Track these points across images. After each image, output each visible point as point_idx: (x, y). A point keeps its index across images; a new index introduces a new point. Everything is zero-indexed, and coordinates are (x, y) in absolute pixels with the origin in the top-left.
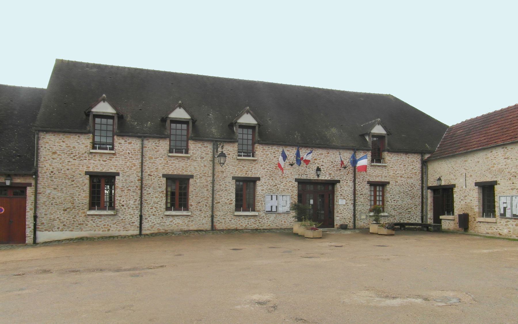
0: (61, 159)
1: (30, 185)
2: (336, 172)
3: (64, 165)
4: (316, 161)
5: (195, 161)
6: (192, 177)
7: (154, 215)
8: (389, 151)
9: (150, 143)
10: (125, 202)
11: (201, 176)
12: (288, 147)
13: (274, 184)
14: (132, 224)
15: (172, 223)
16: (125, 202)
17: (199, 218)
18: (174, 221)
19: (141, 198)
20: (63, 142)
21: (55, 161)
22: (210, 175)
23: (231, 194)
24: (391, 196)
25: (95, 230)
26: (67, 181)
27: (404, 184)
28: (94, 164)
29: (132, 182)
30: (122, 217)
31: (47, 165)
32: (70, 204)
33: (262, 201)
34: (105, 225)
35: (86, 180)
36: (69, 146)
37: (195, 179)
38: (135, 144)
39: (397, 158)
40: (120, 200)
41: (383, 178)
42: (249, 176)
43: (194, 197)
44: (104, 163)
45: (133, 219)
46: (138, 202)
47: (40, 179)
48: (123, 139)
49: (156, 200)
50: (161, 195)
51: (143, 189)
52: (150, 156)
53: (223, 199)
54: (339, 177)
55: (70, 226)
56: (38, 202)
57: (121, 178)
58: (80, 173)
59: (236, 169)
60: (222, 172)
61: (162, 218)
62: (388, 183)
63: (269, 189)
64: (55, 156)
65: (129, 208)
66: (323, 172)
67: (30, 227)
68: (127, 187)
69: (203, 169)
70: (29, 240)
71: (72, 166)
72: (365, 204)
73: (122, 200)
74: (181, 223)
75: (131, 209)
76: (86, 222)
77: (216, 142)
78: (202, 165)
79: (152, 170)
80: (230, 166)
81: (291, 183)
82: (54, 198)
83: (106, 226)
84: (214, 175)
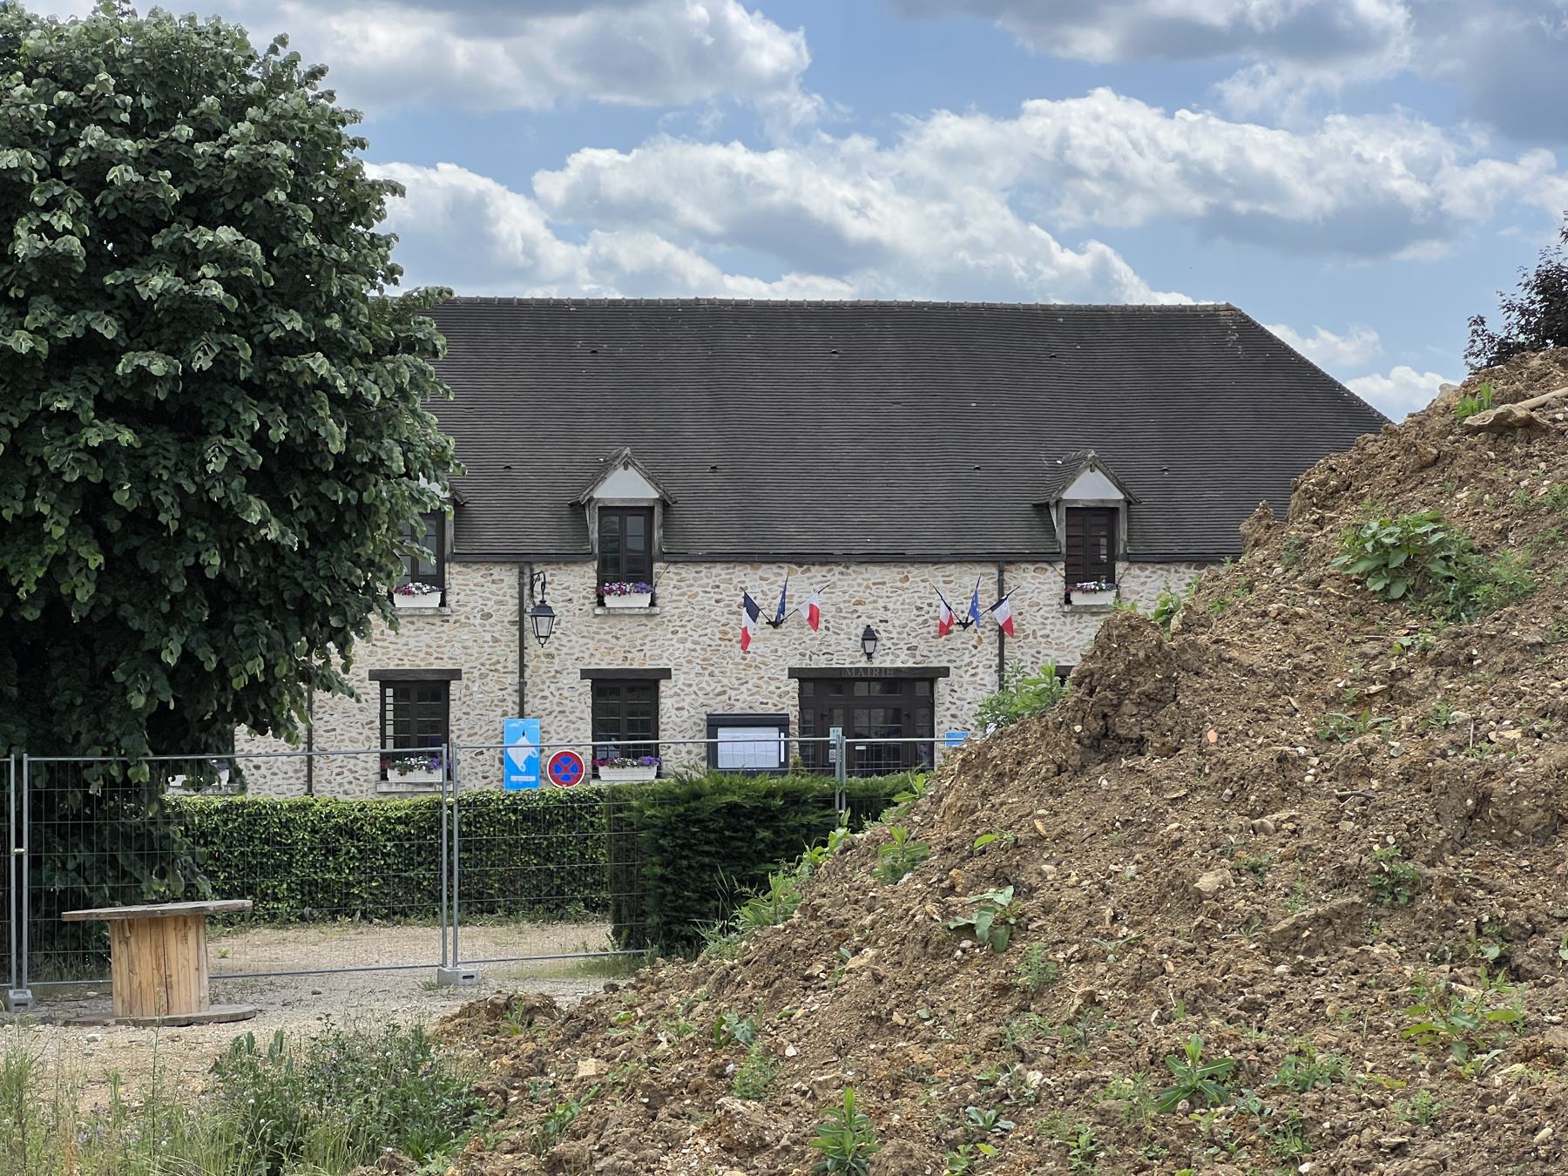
4: (859, 608)
6: (456, 674)
8: (1132, 559)
11: (483, 670)
12: (764, 566)
13: (719, 689)
23: (580, 724)
37: (464, 681)
42: (635, 666)
43: (464, 737)
50: (366, 732)
54: (945, 658)
59: (592, 644)
63: (703, 705)
66: (889, 644)
69: (489, 650)
75: (281, 775)
77: (524, 561)
78: (488, 637)
84: (522, 667)
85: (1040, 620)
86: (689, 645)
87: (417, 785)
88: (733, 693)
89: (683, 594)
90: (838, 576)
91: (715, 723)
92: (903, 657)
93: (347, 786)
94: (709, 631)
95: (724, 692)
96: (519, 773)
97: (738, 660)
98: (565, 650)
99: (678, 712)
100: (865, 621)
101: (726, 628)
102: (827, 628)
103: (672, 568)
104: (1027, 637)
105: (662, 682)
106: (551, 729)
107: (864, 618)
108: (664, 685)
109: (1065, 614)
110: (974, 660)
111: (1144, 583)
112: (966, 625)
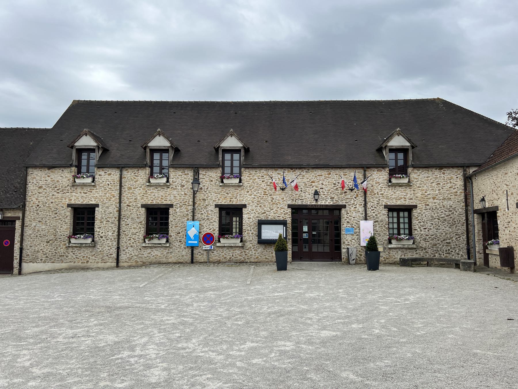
0: (46, 193)
1: (18, 218)
2: (340, 196)
3: (48, 198)
4: (313, 184)
5: (175, 189)
6: (171, 206)
7: (131, 246)
9: (129, 173)
10: (104, 234)
11: (181, 204)
12: (279, 170)
13: (263, 212)
14: (110, 256)
15: (149, 255)
16: (104, 234)
17: (178, 250)
18: (152, 253)
19: (119, 229)
20: (49, 176)
21: (41, 195)
22: (191, 203)
23: (214, 223)
24: (420, 222)
25: (75, 262)
26: (51, 214)
27: (438, 207)
28: (75, 196)
29: (111, 213)
30: (100, 248)
31: (34, 199)
32: (53, 236)
33: (248, 230)
34: (84, 257)
35: (68, 213)
36: (54, 181)
37: (174, 208)
38: (115, 174)
39: (426, 175)
40: (99, 232)
41: (408, 200)
42: (234, 203)
43: (173, 228)
44: (85, 195)
45: (111, 250)
46: (116, 233)
47: (27, 213)
48: (103, 170)
49: (135, 231)
50: (139, 225)
51: (121, 220)
52: (129, 186)
53: (205, 229)
55: (52, 257)
56: (25, 234)
57: (101, 210)
58: (63, 205)
59: (219, 196)
60: (204, 200)
61: (140, 249)
62: (415, 207)
63: (257, 217)
64: (40, 191)
65: (107, 240)
66: (324, 196)
67: (17, 259)
68: (106, 219)
69: (183, 198)
70: (16, 271)
71: (56, 200)
72: (382, 234)
73: (101, 232)
74: (159, 255)
75: (109, 240)
76: (67, 254)
77: (196, 169)
78: (183, 193)
79: (131, 200)
80: (212, 193)
81: (283, 210)
82: (38, 231)
83: (85, 258)
84: (194, 203)
86: (253, 196)
87: (155, 244)
88: (268, 213)
89: (251, 179)
90: (305, 173)
91: (261, 223)
92: (329, 201)
93: (132, 244)
95: (265, 213)
96: (192, 240)
97: (270, 201)
98: (209, 198)
100: (315, 188)
101: (266, 191)
102: (301, 191)
103: (247, 170)
105: (243, 209)
106: (204, 225)
107: (314, 187)
108: (244, 211)
109: (389, 186)
110: (355, 202)
111: (419, 175)
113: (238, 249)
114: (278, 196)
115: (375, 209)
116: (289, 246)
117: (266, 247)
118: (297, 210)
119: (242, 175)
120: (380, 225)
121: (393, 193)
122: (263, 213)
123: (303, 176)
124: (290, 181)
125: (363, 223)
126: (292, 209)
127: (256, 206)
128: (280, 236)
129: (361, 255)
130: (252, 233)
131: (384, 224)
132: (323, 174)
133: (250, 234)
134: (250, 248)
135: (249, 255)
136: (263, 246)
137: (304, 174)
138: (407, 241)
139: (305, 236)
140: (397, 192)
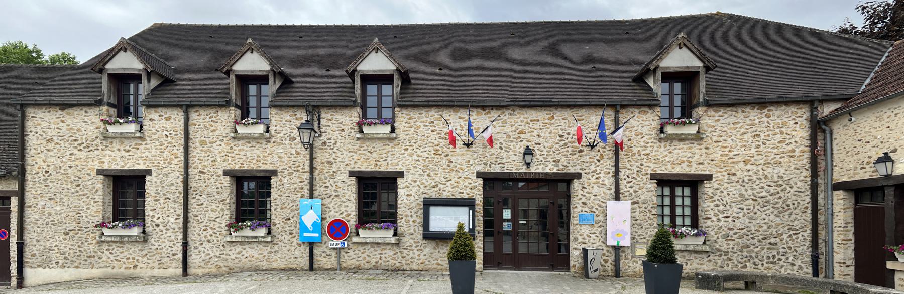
0: (59, 150)
3: (64, 159)
4: (522, 136)
5: (279, 144)
6: (274, 173)
7: (208, 241)
8: (709, 105)
9: (202, 117)
10: (161, 220)
11: (290, 170)
12: (461, 110)
13: (433, 184)
14: (172, 258)
18: (244, 252)
20: (63, 122)
21: (51, 153)
22: (307, 168)
23: (348, 203)
24: (717, 206)
26: (69, 187)
27: (754, 178)
28: (110, 156)
29: (172, 185)
30: (156, 244)
31: (40, 161)
33: (407, 216)
34: (128, 259)
36: (72, 129)
37: (279, 177)
38: (176, 118)
39: (733, 120)
41: (694, 166)
42: (382, 169)
43: (279, 210)
45: (175, 248)
47: (29, 185)
48: (156, 112)
49: (214, 215)
50: (221, 206)
51: (190, 197)
57: (155, 179)
58: (89, 172)
59: (356, 156)
62: (709, 177)
63: (423, 193)
64: (50, 146)
65: (168, 230)
68: (164, 194)
69: (294, 159)
72: (645, 225)
73: (157, 216)
74: (256, 256)
78: (293, 151)
79: (206, 163)
80: (344, 152)
82: (50, 214)
83: (131, 260)
84: (312, 169)
85: (643, 144)
86: (415, 157)
87: (247, 237)
88: (442, 186)
89: (411, 127)
91: (429, 203)
92: (550, 166)
93: (209, 238)
94: (427, 149)
95: (437, 186)
96: (310, 232)
97: (445, 166)
98: (339, 159)
99: (408, 197)
100: (525, 143)
102: (501, 148)
103: (405, 112)
104: (635, 154)
105: (399, 179)
106: (331, 206)
108: (400, 181)
109: (660, 140)
110: (598, 168)
111: (719, 120)
112: (592, 146)
113: (389, 247)
114: (460, 155)
115: (634, 181)
116: (478, 246)
117: (437, 245)
118: (490, 180)
119: (396, 119)
120: (643, 209)
121: (667, 153)
122: (433, 187)
123: (505, 122)
124: (481, 130)
125: (612, 204)
126: (484, 179)
127: (420, 175)
128: (460, 227)
129: (606, 261)
130: (414, 221)
131: (649, 208)
132: (539, 118)
133: (411, 223)
134: (411, 246)
135: (408, 257)
136: (433, 243)
137: (505, 118)
138: (694, 238)
139: (506, 227)
140: (676, 151)
